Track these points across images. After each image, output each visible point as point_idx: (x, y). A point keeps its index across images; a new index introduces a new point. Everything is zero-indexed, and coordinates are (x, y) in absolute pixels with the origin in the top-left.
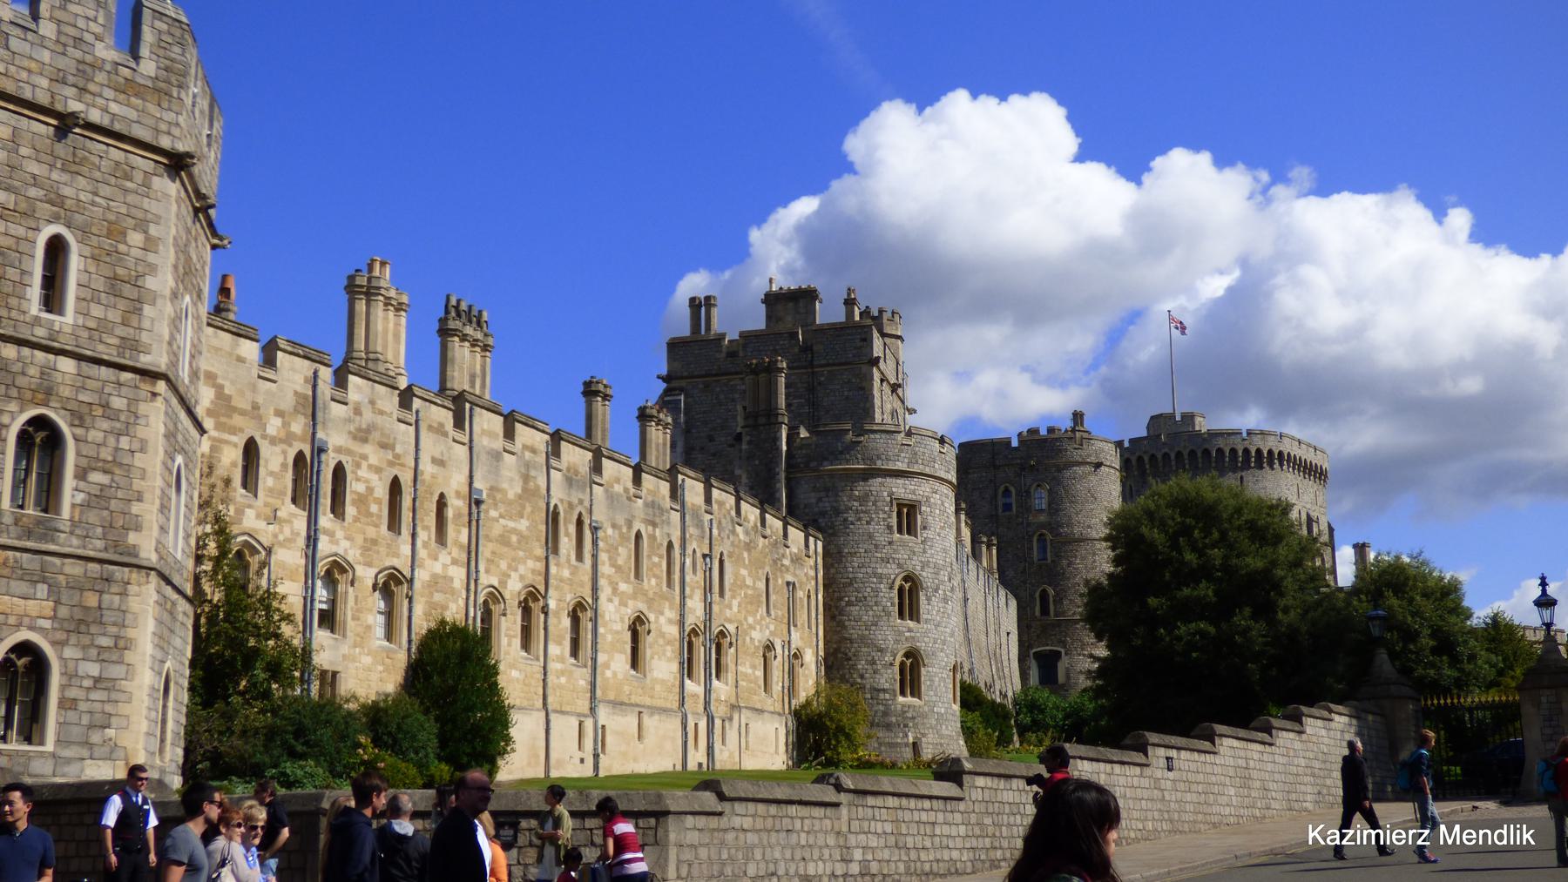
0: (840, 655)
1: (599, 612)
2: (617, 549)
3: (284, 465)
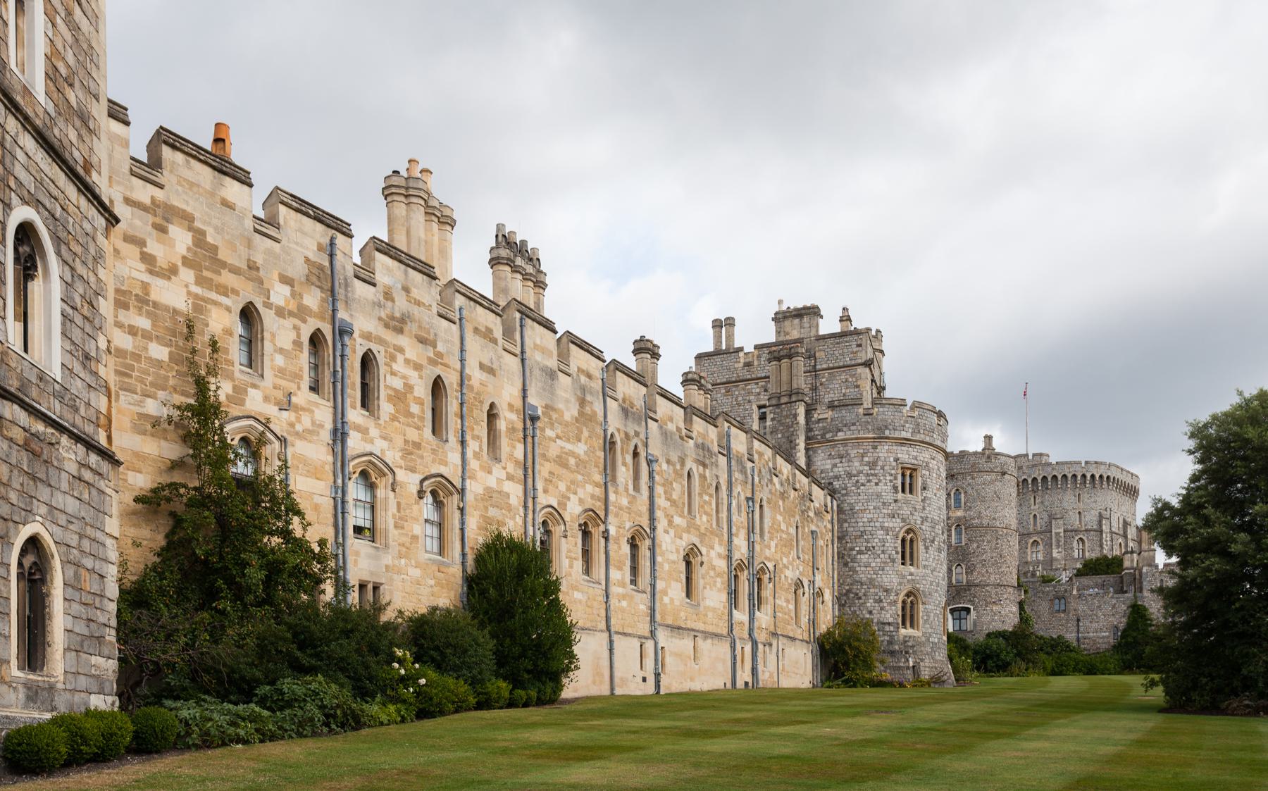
1: (657, 541)
2: (671, 484)
3: (297, 344)
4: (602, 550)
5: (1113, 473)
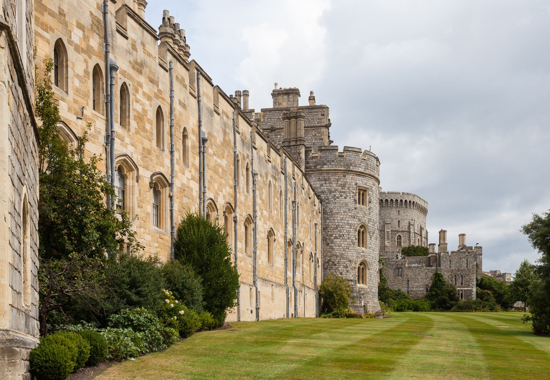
0: (331, 263)
4: (233, 229)
5: (416, 200)
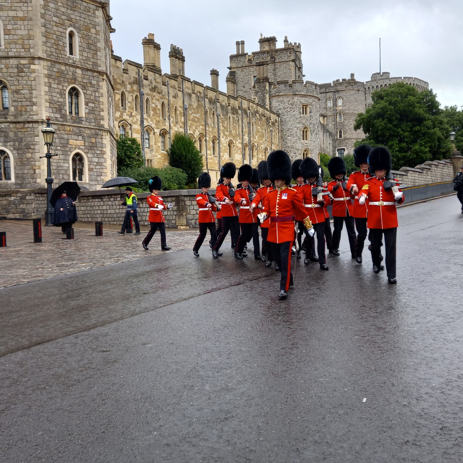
1: (220, 141)
3: (133, 99)
4: (205, 145)
